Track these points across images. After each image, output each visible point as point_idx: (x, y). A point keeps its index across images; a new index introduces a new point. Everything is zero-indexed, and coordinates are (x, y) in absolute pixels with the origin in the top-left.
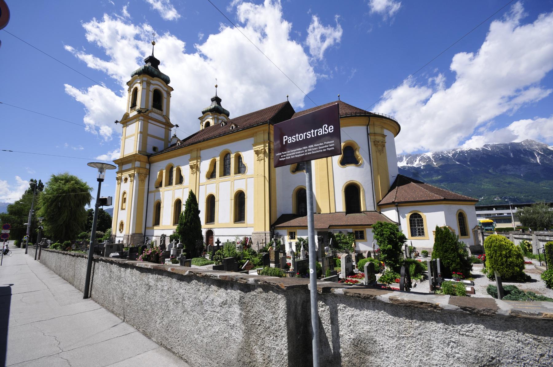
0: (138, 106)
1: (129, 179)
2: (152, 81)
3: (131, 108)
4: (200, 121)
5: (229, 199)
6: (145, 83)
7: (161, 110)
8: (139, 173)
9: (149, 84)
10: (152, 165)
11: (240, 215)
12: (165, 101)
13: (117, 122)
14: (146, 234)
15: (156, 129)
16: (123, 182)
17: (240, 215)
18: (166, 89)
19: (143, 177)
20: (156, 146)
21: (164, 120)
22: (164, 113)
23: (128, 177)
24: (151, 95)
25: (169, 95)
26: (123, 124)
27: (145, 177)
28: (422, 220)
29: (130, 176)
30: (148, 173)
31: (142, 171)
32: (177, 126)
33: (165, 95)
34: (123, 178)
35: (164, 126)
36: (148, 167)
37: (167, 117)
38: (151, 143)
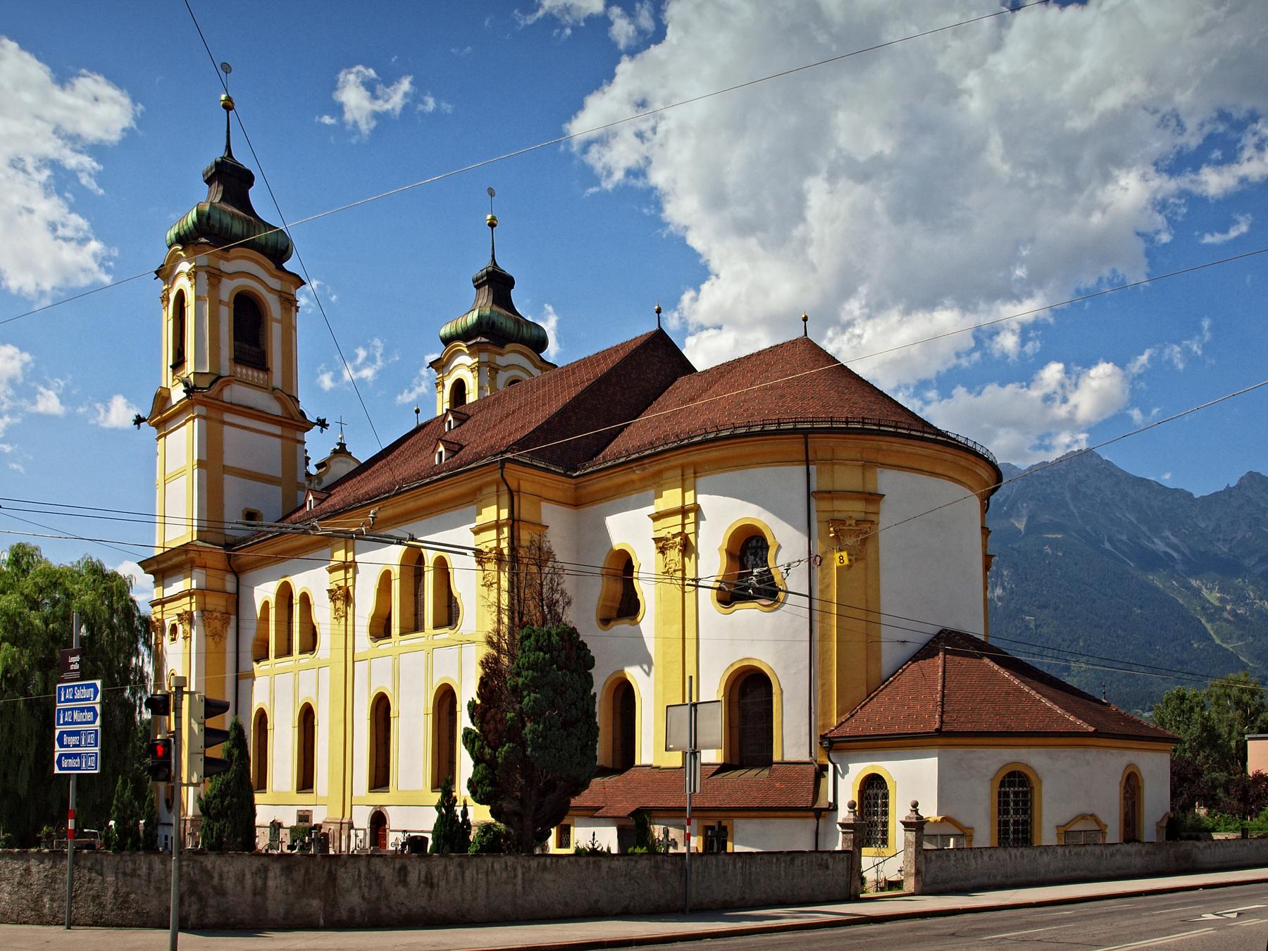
0: (190, 367)
2: (226, 266)
5: (422, 711)
6: (203, 276)
8: (203, 610)
9: (215, 276)
10: (243, 577)
12: (275, 332)
15: (251, 446)
18: (275, 284)
19: (217, 624)
21: (275, 409)
24: (226, 314)
25: (289, 303)
27: (226, 623)
28: (886, 796)
30: (232, 609)
33: (273, 306)
35: (277, 430)
36: (230, 586)
38: (236, 496)
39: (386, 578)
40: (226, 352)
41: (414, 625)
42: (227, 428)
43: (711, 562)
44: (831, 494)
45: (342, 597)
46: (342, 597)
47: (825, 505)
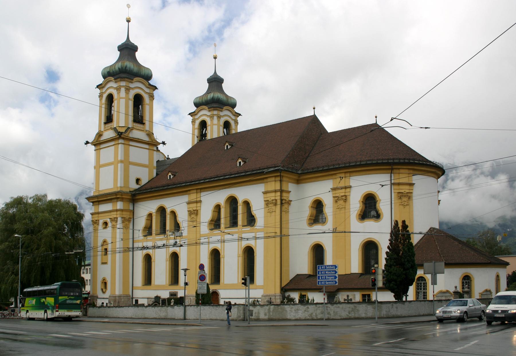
1: (110, 224)
3: (105, 123)
4: (190, 118)
7: (144, 124)
10: (136, 205)
11: (249, 275)
13: (87, 143)
14: (134, 297)
16: (101, 226)
17: (249, 275)
20: (138, 177)
21: (146, 139)
22: (147, 127)
23: (108, 221)
26: (95, 145)
29: (112, 220)
30: (132, 217)
31: (127, 215)
32: (164, 143)
34: (101, 222)
36: (131, 208)
37: (150, 134)
39: (218, 207)
40: (131, 118)
41: (234, 223)
42: (131, 147)
43: (355, 204)
44: (399, 184)
45: (194, 213)
46: (194, 213)
47: (396, 187)
